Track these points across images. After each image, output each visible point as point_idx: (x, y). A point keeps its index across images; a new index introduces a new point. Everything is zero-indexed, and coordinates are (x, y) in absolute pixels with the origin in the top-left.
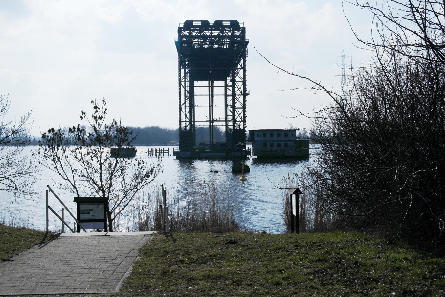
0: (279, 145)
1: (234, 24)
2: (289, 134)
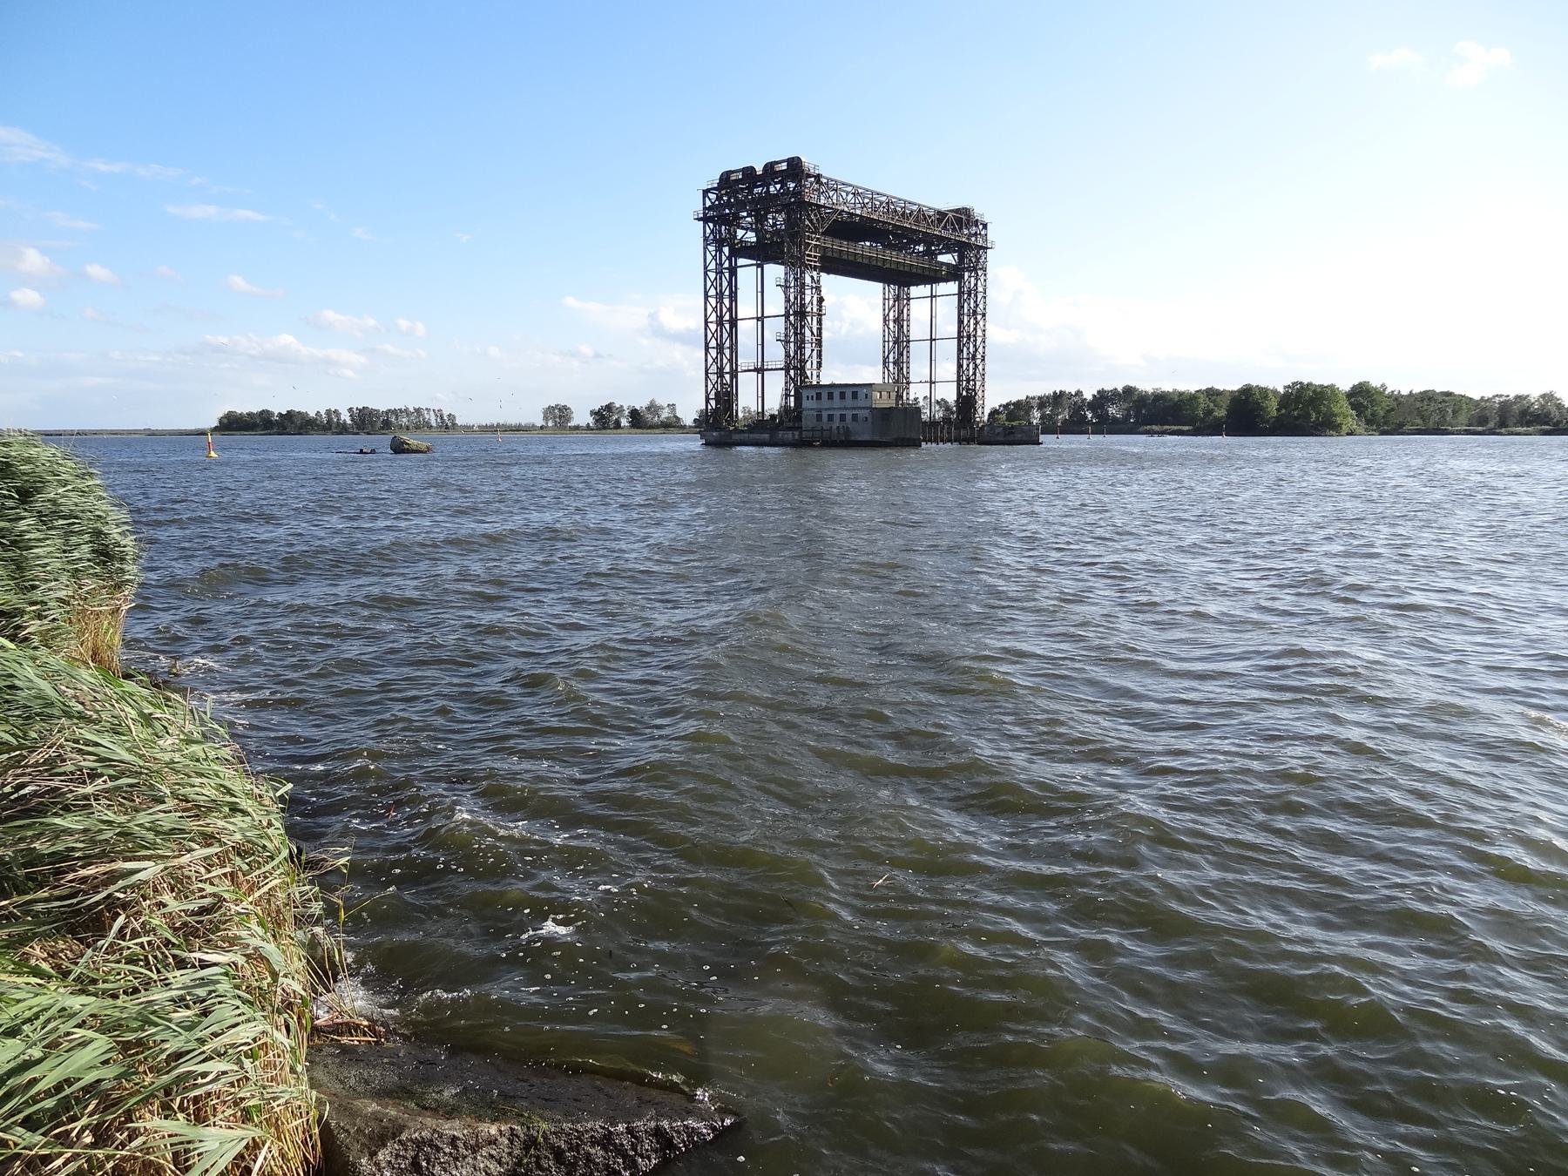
0: (843, 417)
1: (795, 165)
2: (861, 395)
